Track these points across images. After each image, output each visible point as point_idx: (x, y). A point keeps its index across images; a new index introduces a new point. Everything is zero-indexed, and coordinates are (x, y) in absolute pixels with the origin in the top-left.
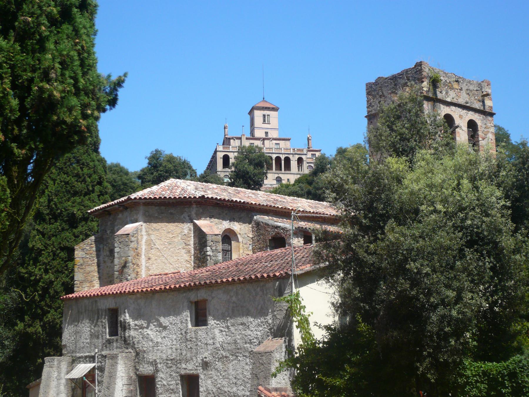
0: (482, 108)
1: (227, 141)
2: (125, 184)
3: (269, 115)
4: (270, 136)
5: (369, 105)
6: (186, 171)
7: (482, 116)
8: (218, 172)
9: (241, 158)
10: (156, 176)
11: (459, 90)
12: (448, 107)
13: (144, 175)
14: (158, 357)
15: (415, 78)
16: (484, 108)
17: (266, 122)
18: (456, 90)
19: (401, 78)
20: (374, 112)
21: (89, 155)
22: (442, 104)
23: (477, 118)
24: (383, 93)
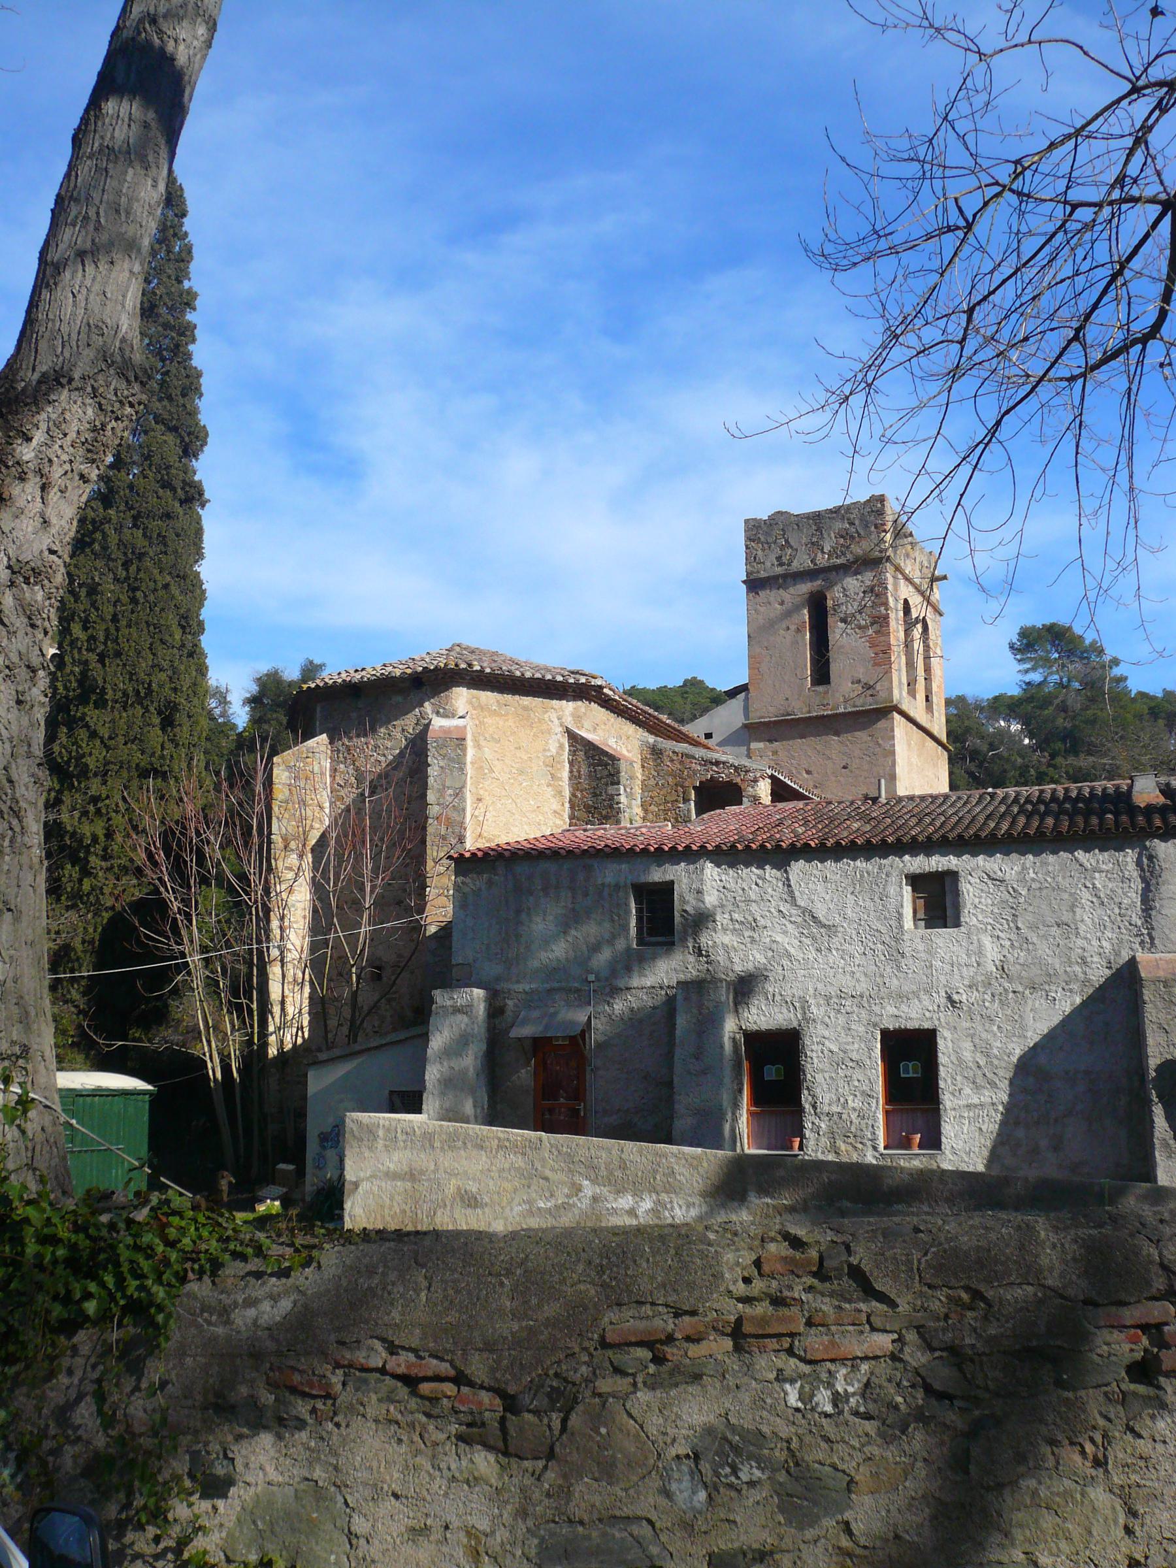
5: (751, 558)
14: (811, 991)
20: (763, 574)
24: (787, 541)
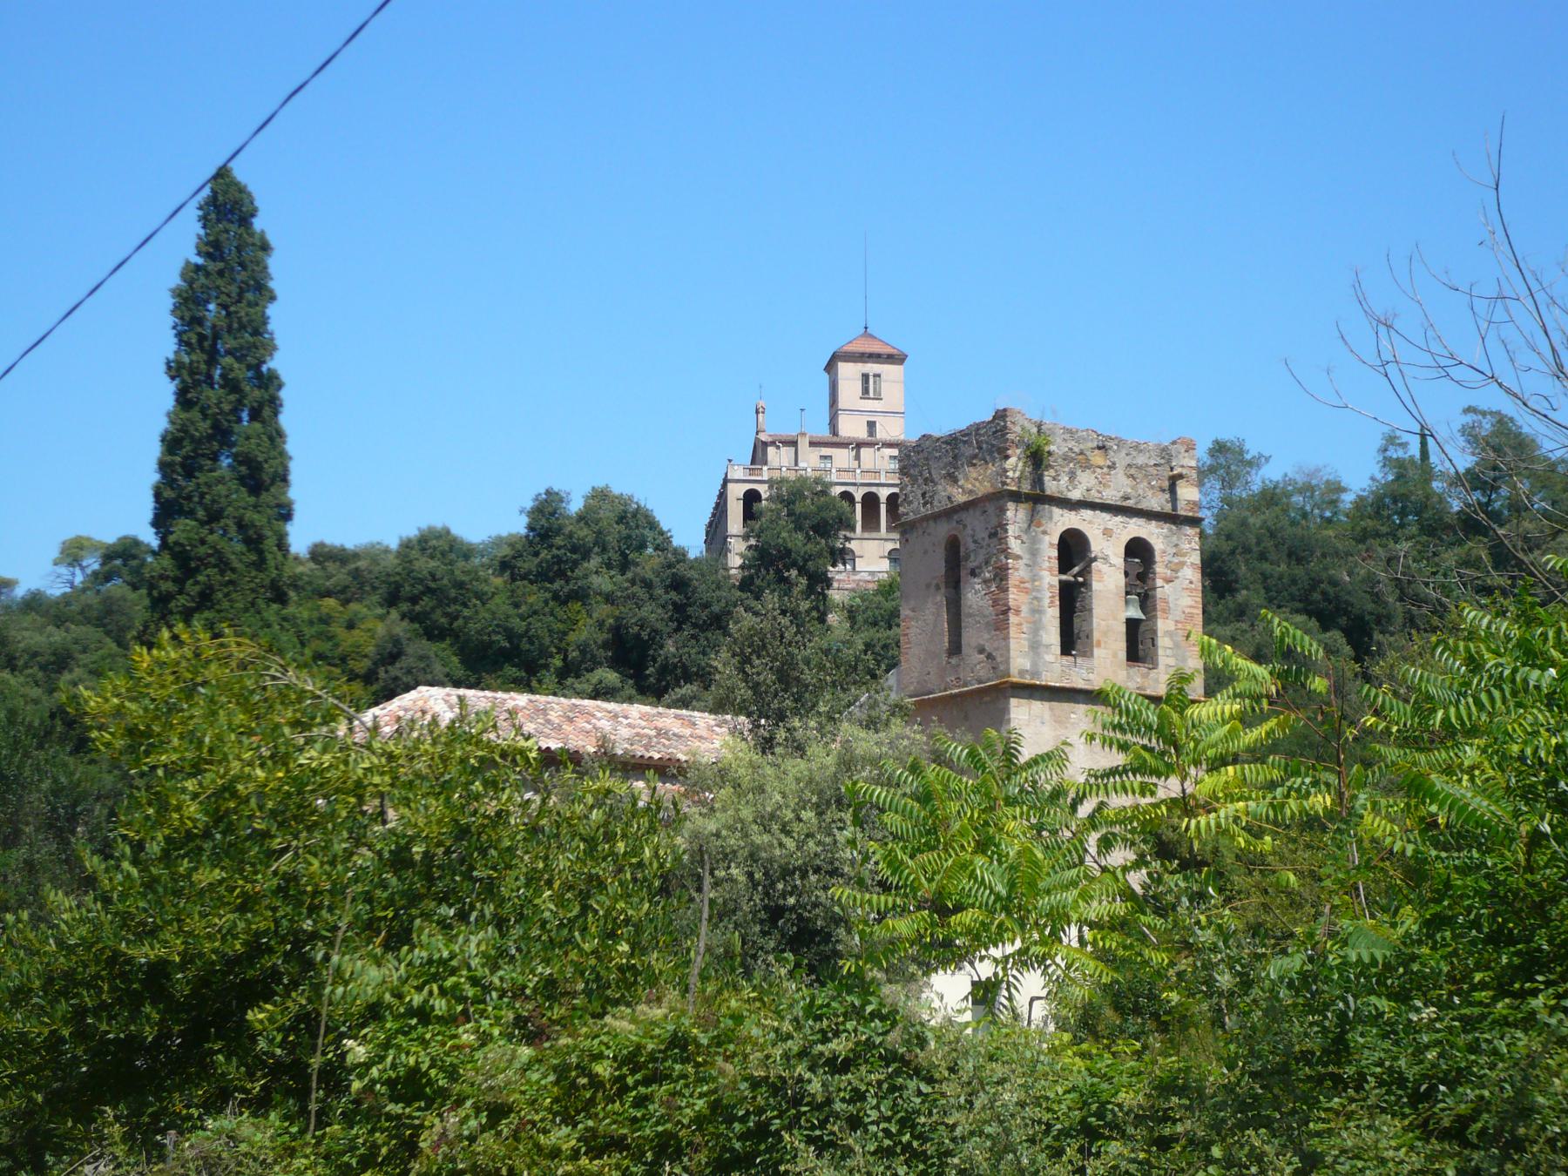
0: (1168, 508)
1: (759, 454)
2: (460, 585)
3: (879, 376)
4: (881, 434)
6: (643, 535)
7: (1166, 528)
8: (731, 536)
9: (772, 511)
10: (547, 562)
11: (1105, 470)
12: (1073, 513)
13: (514, 558)
15: (993, 446)
16: (1174, 508)
17: (871, 395)
18: (1099, 470)
19: (965, 442)
21: (259, 613)
22: (1057, 506)
23: (1154, 533)
